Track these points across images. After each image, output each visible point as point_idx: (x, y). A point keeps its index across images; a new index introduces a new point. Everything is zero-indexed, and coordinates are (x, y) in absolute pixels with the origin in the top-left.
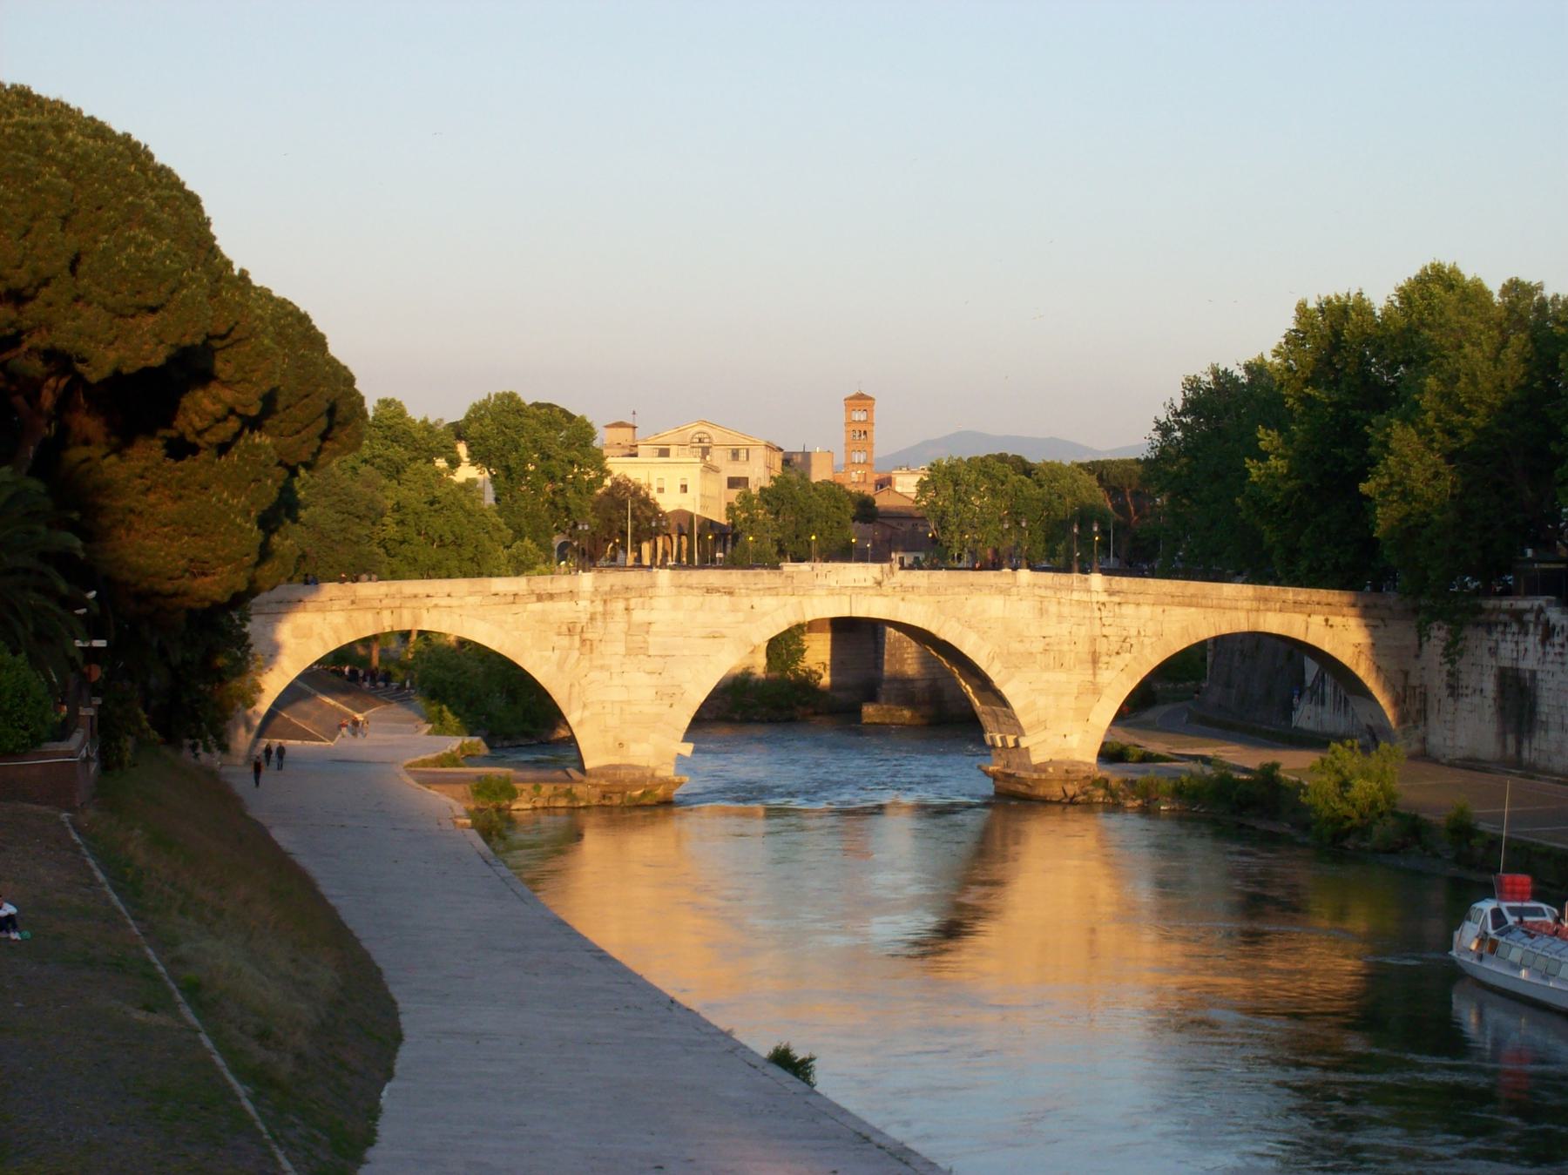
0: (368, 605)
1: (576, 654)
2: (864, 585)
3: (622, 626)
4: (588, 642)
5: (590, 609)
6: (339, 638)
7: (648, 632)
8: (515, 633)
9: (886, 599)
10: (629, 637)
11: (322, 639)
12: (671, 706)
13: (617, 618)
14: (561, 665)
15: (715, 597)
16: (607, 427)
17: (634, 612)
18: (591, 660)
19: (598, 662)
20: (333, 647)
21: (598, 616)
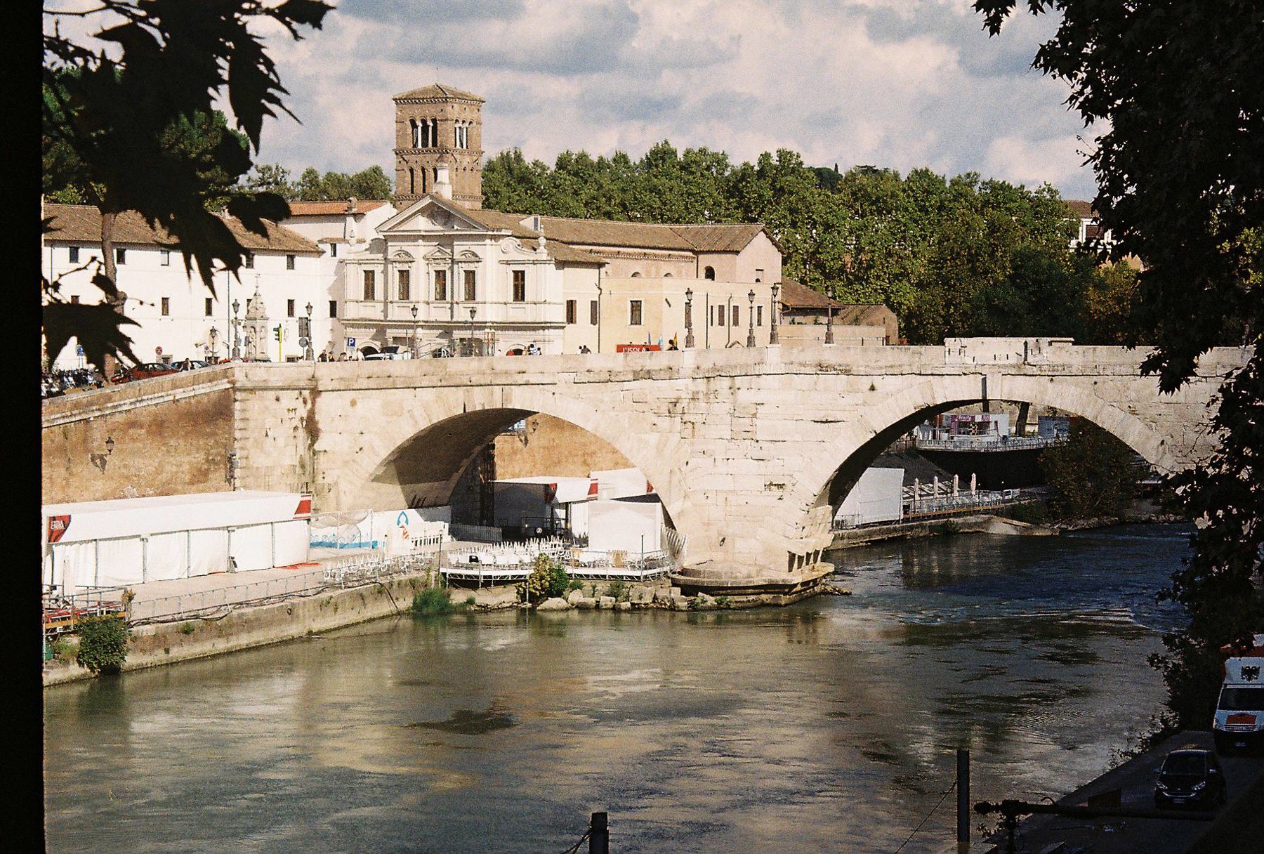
2: (1007, 362)
3: (728, 407)
7: (755, 415)
8: (612, 414)
11: (412, 417)
15: (830, 380)
18: (693, 444)
20: (424, 424)
21: (701, 396)
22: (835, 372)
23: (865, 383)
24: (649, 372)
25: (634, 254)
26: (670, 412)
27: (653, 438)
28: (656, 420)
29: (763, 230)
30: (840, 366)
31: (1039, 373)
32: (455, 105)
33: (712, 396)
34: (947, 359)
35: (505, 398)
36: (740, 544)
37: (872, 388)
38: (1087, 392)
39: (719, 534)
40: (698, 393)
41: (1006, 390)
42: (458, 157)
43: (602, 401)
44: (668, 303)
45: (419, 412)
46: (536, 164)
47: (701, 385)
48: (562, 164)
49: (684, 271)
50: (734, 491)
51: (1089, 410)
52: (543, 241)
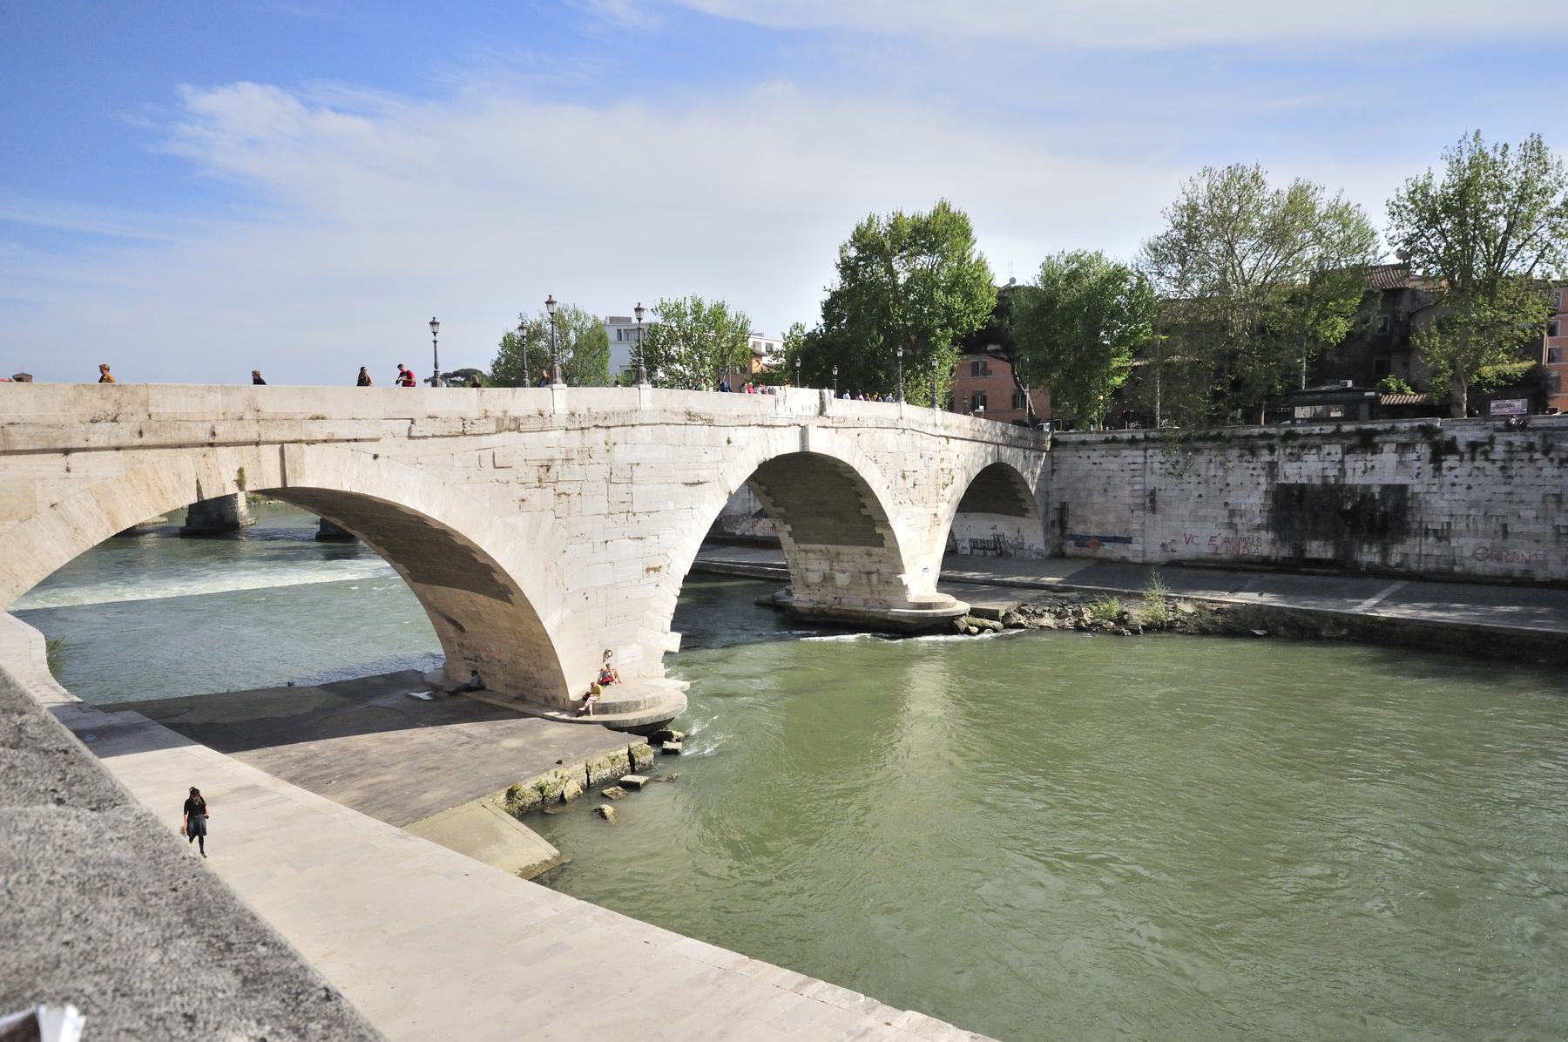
10: (611, 486)
13: (596, 458)
22: (700, 422)
23: (724, 433)
26: (540, 481)
28: (523, 493)
40: (571, 450)
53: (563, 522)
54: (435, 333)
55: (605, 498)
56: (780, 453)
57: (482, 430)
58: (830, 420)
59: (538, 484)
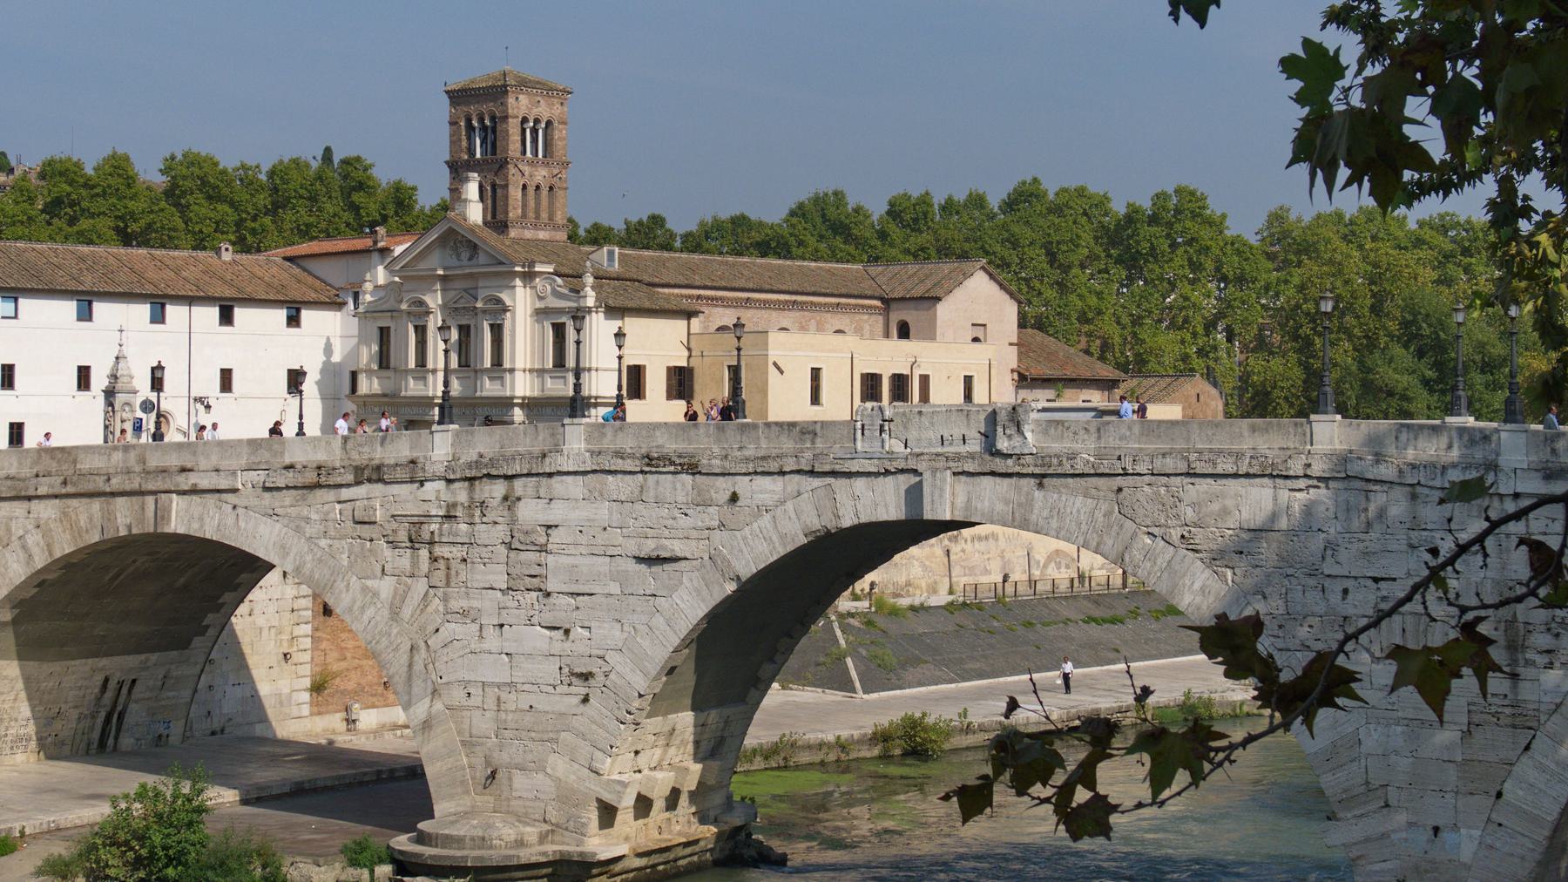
0: (89, 486)
1: (421, 586)
2: (963, 449)
3: (501, 532)
4: (442, 564)
5: (446, 496)
6: (49, 546)
8: (323, 543)
9: (1007, 481)
10: (513, 554)
11: (24, 547)
12: (586, 700)
14: (395, 613)
16: (1287, 167)
17: (521, 504)
19: (455, 605)
22: (672, 468)
23: (723, 487)
24: (378, 468)
25: (737, 300)
26: (411, 541)
27: (386, 587)
28: (387, 552)
29: (983, 268)
30: (680, 457)
31: (1017, 469)
32: (521, 97)
33: (478, 513)
34: (859, 444)
35: (161, 515)
36: (520, 781)
37: (734, 498)
38: (1104, 507)
39: (488, 763)
40: (454, 505)
41: (961, 500)
42: (526, 169)
43: (307, 520)
44: (778, 368)
45: (34, 539)
46: (857, 210)
47: (461, 493)
48: (894, 212)
49: (867, 327)
50: (511, 685)
51: (1110, 542)
52: (589, 279)
53: (440, 592)
54: (739, 338)
55: (502, 568)
56: (865, 518)
57: (339, 480)
58: (1010, 462)
59: (408, 544)
